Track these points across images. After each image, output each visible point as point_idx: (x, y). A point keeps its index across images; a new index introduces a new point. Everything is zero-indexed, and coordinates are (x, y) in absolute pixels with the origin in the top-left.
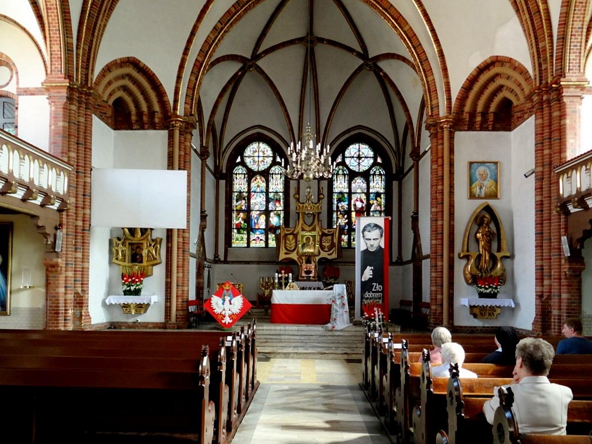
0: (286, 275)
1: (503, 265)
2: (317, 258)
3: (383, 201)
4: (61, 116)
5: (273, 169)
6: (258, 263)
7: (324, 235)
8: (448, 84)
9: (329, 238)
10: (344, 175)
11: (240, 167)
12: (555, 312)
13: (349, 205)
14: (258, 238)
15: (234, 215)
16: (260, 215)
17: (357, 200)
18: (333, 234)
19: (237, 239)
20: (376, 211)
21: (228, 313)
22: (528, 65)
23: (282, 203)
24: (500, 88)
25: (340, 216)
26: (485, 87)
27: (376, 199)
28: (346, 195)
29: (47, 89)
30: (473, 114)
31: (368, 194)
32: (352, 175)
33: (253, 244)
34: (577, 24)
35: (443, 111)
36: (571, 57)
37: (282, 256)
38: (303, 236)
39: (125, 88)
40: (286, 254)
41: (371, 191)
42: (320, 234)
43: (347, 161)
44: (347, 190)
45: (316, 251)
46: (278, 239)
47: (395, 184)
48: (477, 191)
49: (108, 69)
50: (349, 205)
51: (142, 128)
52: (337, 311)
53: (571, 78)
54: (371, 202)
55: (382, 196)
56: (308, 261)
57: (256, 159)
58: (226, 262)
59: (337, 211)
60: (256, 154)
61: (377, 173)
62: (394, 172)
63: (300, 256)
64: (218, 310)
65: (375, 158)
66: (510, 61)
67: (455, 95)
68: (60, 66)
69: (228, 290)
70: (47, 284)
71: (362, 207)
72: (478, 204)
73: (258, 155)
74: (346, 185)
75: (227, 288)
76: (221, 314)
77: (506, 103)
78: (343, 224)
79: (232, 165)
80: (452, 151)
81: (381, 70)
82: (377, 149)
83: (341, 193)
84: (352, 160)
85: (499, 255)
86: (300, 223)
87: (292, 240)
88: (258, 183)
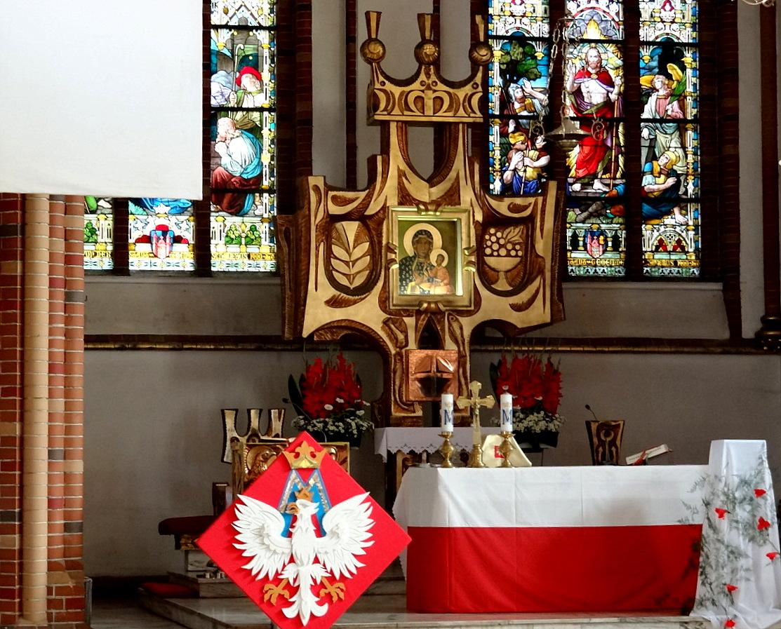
0: (490, 401)
2: (468, 325)
3: (691, 78)
6: (178, 342)
7: (494, 220)
9: (515, 234)
14: (164, 229)
17: (584, 73)
18: (531, 218)
20: (662, 121)
21: (307, 574)
23: (266, 76)
25: (517, 139)
27: (663, 71)
28: (540, 52)
31: (629, 46)
33: (139, 259)
37: (318, 313)
40: (334, 303)
41: (646, 33)
42: (479, 217)
52: (735, 553)
54: (644, 81)
55: (688, 58)
56: (430, 339)
59: (504, 118)
63: (394, 316)
64: (263, 563)
69: (305, 473)
71: (608, 104)
75: (304, 464)
76: (277, 580)
78: (531, 173)
83: (519, 39)
86: (393, 172)
87: (357, 242)
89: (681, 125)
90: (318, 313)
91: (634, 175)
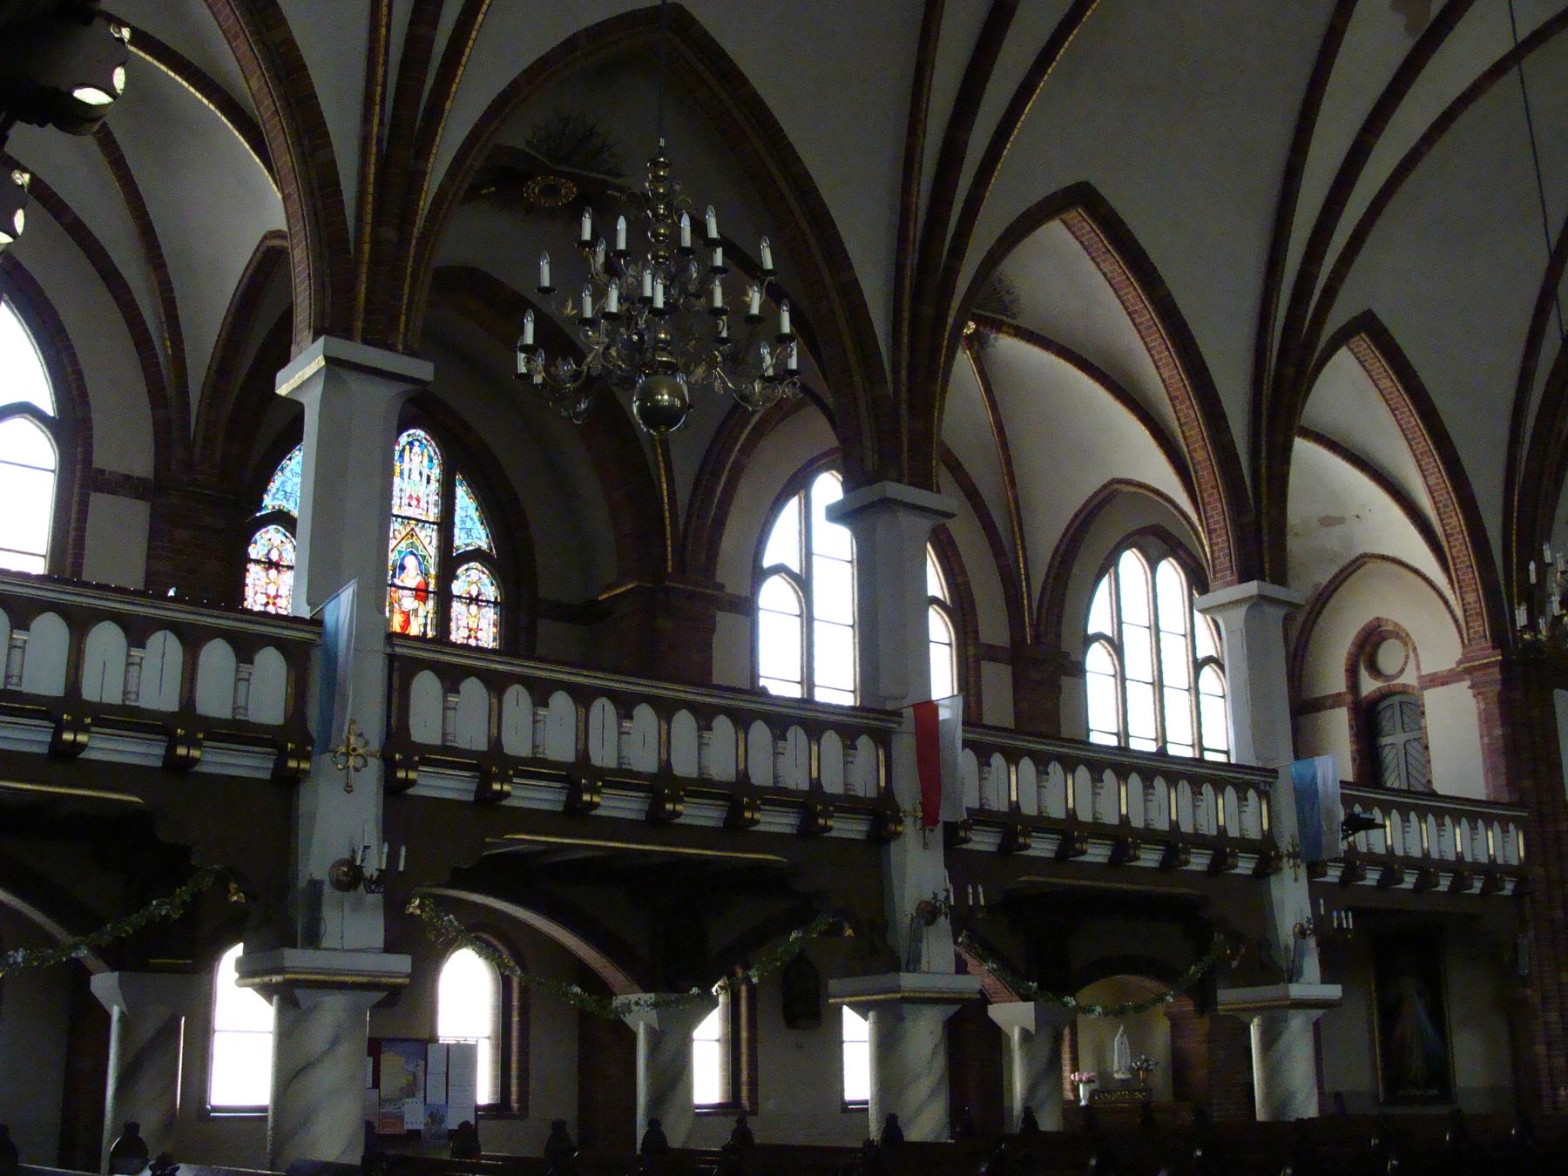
4: (1497, 716)
29: (1469, 671)
68: (1481, 627)
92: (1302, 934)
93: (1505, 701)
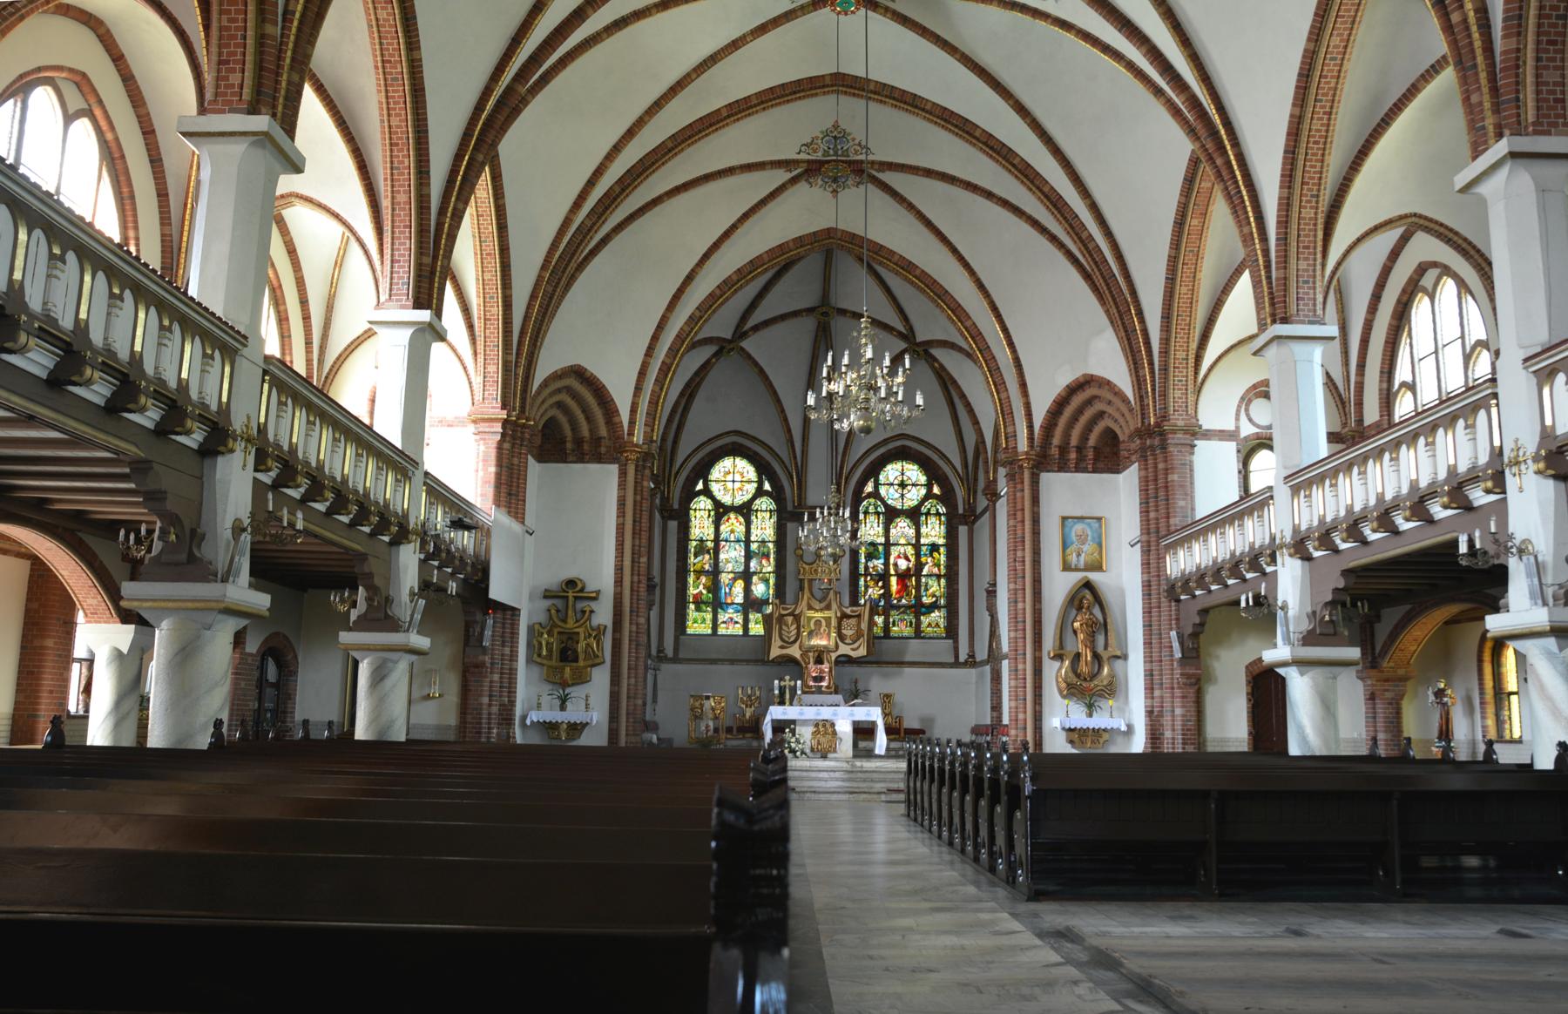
1: (1111, 669)
2: (834, 656)
3: (943, 559)
5: (757, 502)
7: (845, 616)
8: (1028, 406)
9: (853, 621)
10: (878, 514)
11: (702, 498)
12: (1168, 734)
13: (886, 564)
15: (691, 580)
16: (734, 579)
19: (695, 621)
22: (1129, 393)
24: (1101, 415)
26: (1080, 411)
29: (475, 422)
30: (1064, 449)
31: (917, 546)
32: (891, 514)
33: (722, 630)
34: (1181, 355)
35: (1023, 445)
36: (1175, 394)
37: (775, 652)
38: (810, 619)
39: (560, 405)
40: (782, 647)
41: (923, 541)
43: (883, 491)
44: (882, 540)
45: (832, 643)
46: (767, 621)
47: (963, 530)
48: (1073, 559)
49: (545, 384)
50: (886, 564)
51: (581, 460)
53: (1178, 420)
55: (942, 550)
56: (819, 661)
57: (730, 485)
58: (676, 659)
60: (730, 477)
61: (933, 511)
62: (961, 511)
63: (805, 653)
65: (929, 486)
66: (1109, 383)
67: (1039, 419)
68: (495, 391)
70: (465, 691)
71: (908, 569)
72: (1075, 578)
73: (733, 478)
74: (881, 530)
77: (1110, 437)
79: (689, 495)
80: (1035, 500)
81: (936, 360)
82: (933, 473)
83: (873, 544)
84: (891, 490)
85: (1105, 655)
88: (733, 526)
89: (939, 577)
90: (775, 652)
91: (918, 597)
92: (412, 594)
93: (500, 448)
